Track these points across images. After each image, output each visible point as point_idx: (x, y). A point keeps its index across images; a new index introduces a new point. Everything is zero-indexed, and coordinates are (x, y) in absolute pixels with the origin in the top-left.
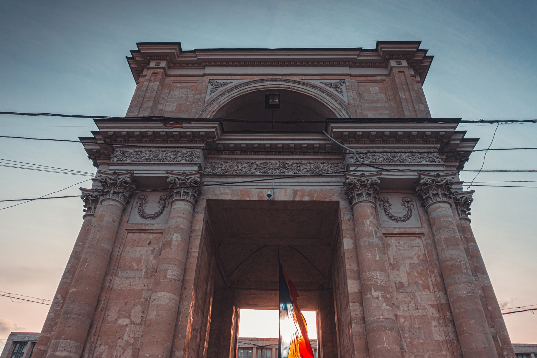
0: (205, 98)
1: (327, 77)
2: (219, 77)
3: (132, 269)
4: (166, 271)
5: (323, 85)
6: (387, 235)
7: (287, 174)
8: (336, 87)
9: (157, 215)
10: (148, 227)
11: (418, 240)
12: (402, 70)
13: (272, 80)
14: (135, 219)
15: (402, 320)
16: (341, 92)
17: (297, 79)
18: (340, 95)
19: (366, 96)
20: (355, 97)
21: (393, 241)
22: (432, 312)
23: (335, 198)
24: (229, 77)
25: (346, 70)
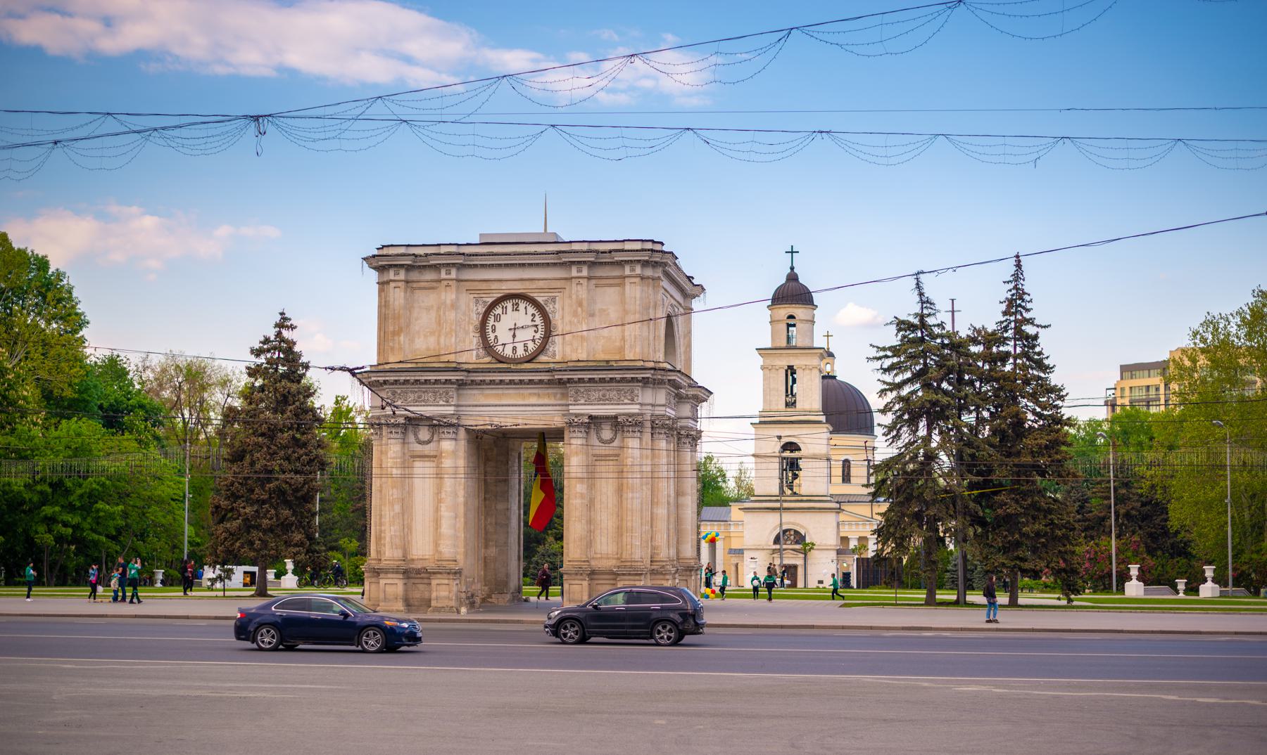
9: (429, 442)
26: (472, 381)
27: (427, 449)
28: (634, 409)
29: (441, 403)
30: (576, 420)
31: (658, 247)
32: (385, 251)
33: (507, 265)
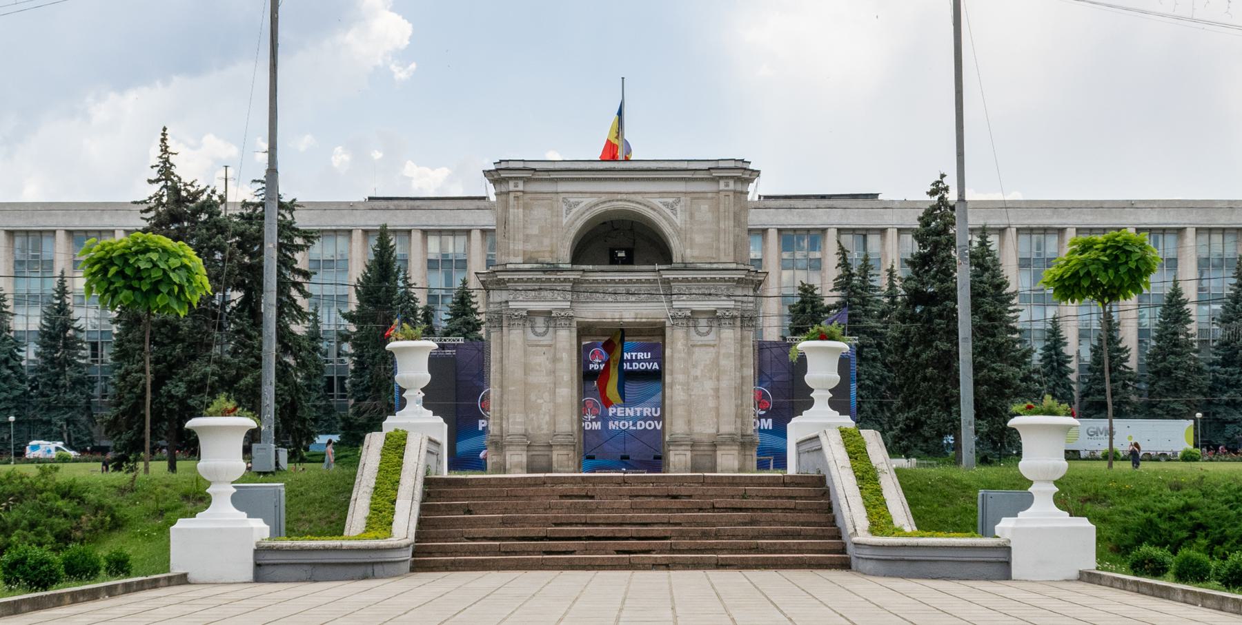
0: (562, 222)
1: (665, 195)
2: (571, 195)
3: (537, 371)
4: (563, 376)
5: (661, 205)
6: (693, 346)
7: (630, 300)
8: (673, 210)
9: (545, 333)
10: (541, 343)
11: (712, 348)
12: (727, 193)
13: (618, 200)
14: (532, 336)
15: (693, 397)
16: (675, 215)
17: (639, 198)
18: (674, 217)
19: (697, 216)
20: (688, 219)
21: (696, 350)
22: (711, 392)
23: (662, 320)
24: (580, 195)
25: (680, 187)
26: (586, 280)
27: (546, 340)
28: (731, 304)
29: (559, 298)
30: (727, 314)
31: (745, 166)
32: (503, 165)
33: (621, 179)
